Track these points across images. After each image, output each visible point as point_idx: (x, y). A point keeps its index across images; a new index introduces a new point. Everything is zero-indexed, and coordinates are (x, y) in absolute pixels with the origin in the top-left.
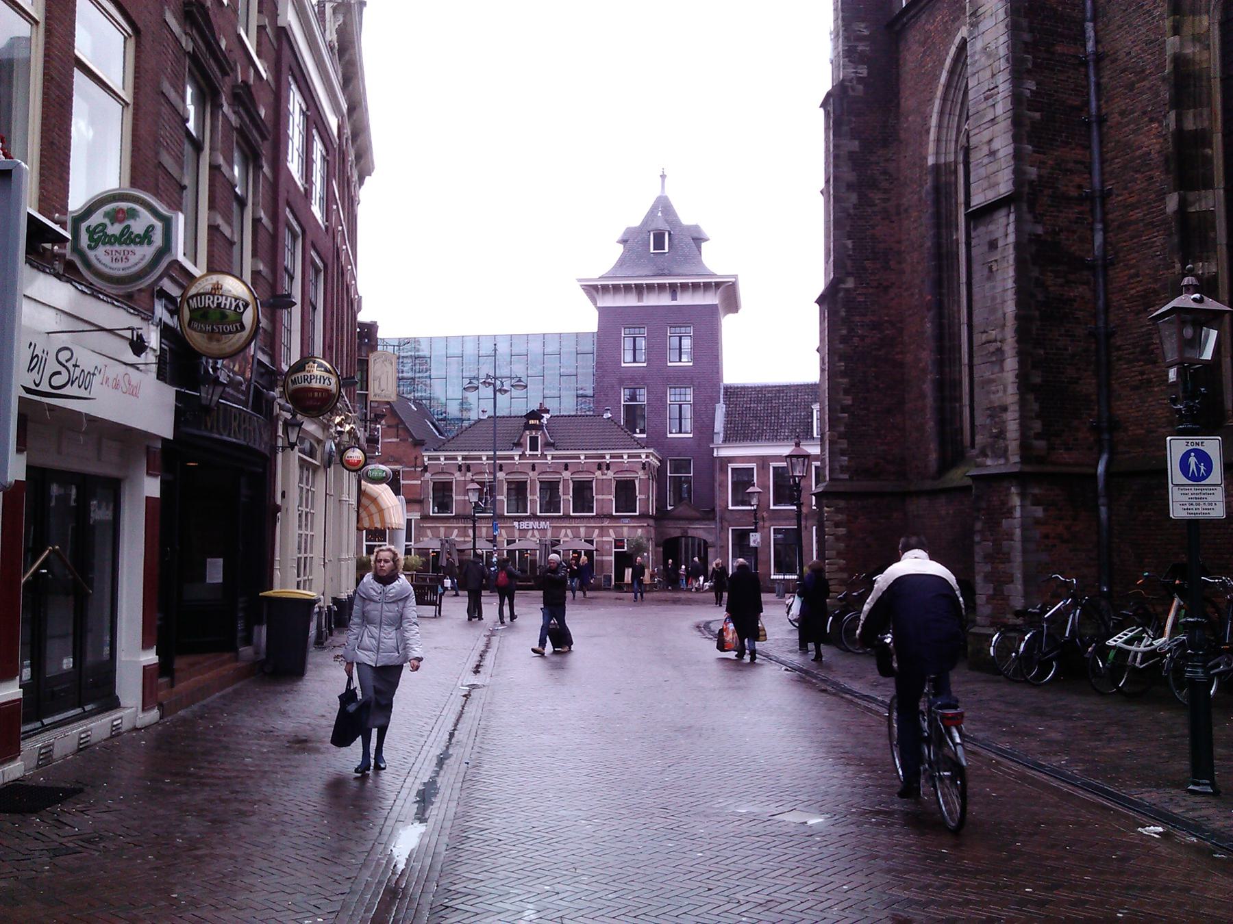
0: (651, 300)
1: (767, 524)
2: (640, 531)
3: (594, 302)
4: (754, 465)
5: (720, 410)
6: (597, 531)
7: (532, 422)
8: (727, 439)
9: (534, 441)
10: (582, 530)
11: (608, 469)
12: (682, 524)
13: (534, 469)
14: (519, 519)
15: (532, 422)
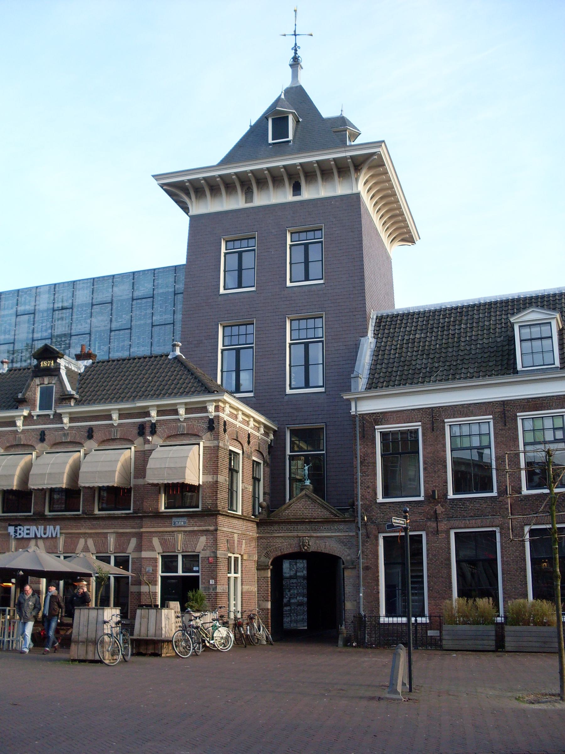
0: (262, 199)
1: (442, 526)
2: (203, 539)
3: (186, 209)
4: (417, 425)
5: (368, 344)
6: (133, 542)
7: (44, 364)
8: (372, 385)
9: (46, 394)
10: (111, 540)
11: (153, 432)
12: (302, 532)
13: (42, 440)
14: (16, 522)
15: (44, 364)
